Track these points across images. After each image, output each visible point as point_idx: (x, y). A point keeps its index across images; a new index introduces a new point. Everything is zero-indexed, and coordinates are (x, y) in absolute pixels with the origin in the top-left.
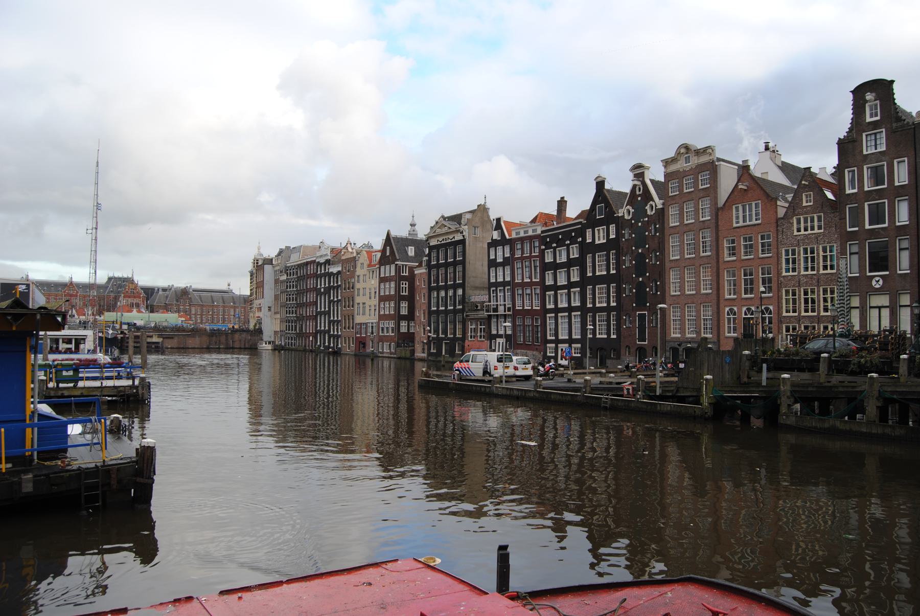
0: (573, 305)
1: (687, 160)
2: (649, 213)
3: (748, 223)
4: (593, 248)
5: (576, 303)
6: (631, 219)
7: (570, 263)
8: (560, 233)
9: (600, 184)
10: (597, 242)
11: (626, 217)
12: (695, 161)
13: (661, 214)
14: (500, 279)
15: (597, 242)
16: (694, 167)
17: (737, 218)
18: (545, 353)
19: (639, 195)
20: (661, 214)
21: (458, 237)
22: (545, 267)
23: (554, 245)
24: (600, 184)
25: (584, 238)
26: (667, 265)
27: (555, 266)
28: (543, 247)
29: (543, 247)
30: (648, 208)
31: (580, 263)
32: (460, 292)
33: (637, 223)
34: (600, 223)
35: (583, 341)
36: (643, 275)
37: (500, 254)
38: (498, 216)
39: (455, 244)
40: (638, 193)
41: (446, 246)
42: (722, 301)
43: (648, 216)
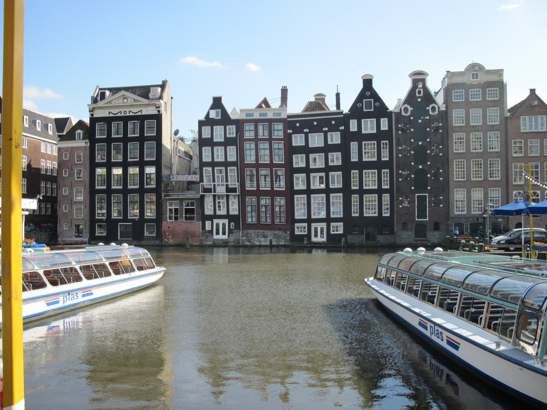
0: (331, 187)
1: (475, 76)
2: (431, 113)
3: (540, 130)
4: (359, 137)
5: (338, 184)
6: (410, 116)
7: (327, 149)
8: (315, 120)
9: (368, 83)
10: (364, 132)
11: (403, 113)
12: (482, 78)
13: (445, 116)
14: (221, 159)
15: (364, 132)
16: (482, 82)
17: (525, 125)
18: (293, 231)
19: (419, 97)
20: (445, 116)
21: (152, 111)
22: (291, 151)
23: (306, 130)
24: (368, 83)
25: (347, 126)
26: (451, 157)
27: (306, 150)
28: (290, 131)
29: (290, 131)
30: (429, 108)
31: (344, 148)
32: (150, 170)
33: (416, 119)
34: (368, 115)
35: (347, 219)
36: (424, 163)
37: (219, 134)
38: (217, 95)
39: (142, 118)
40: (417, 95)
41: (125, 119)
42: (510, 187)
43: (430, 115)
